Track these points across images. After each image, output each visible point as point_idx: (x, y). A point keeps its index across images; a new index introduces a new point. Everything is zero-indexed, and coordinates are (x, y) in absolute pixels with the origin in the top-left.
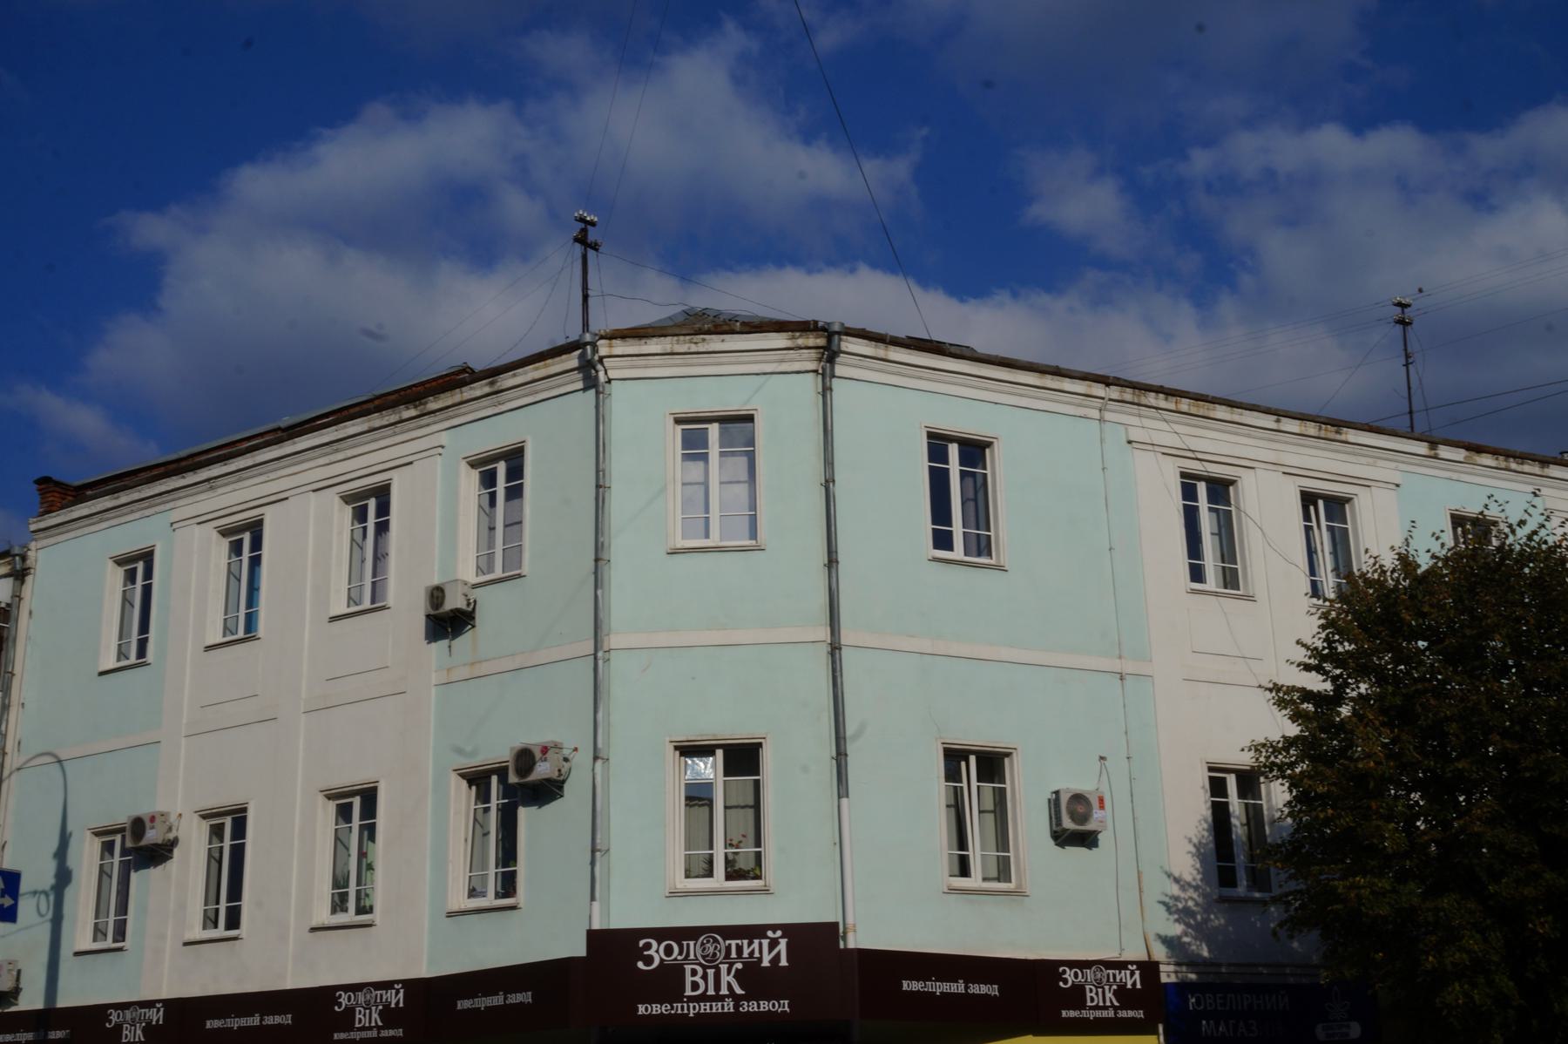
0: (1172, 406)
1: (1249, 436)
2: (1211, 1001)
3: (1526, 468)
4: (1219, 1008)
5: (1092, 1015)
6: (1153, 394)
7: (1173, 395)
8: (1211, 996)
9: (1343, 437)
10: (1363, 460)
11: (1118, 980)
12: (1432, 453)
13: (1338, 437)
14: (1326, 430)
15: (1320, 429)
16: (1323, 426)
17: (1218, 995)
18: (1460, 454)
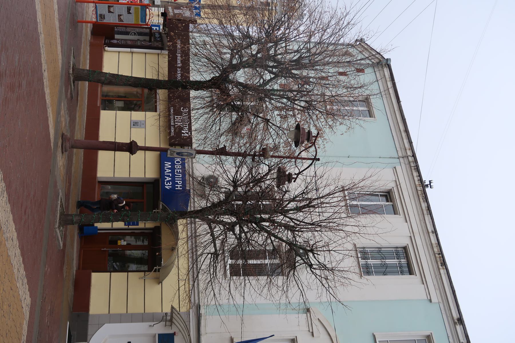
1: (420, 221)
2: (178, 167)
4: (176, 170)
5: (172, 117)
8: (180, 167)
9: (440, 267)
10: (435, 283)
11: (185, 128)
12: (456, 321)
14: (440, 257)
15: (439, 254)
16: (441, 255)
17: (181, 170)
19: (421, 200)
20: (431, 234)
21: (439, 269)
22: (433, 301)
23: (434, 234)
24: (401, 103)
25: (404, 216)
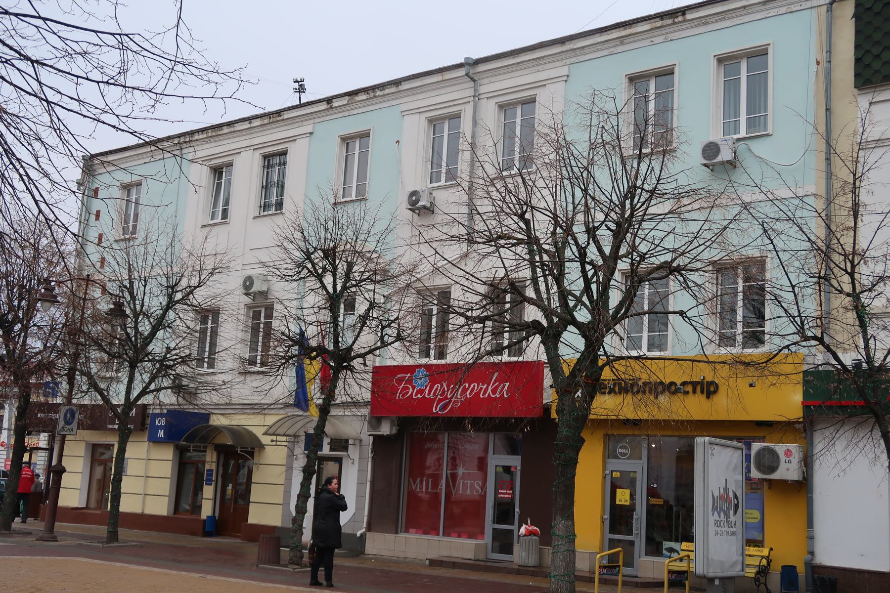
0: (205, 136)
3: (387, 91)
6: (197, 134)
7: (204, 131)
9: (281, 118)
12: (329, 106)
13: (281, 118)
14: (273, 117)
18: (345, 101)
19: (221, 133)
20: (253, 125)
21: (283, 120)
22: (311, 131)
23: (252, 121)
24: (130, 145)
25: (235, 156)
